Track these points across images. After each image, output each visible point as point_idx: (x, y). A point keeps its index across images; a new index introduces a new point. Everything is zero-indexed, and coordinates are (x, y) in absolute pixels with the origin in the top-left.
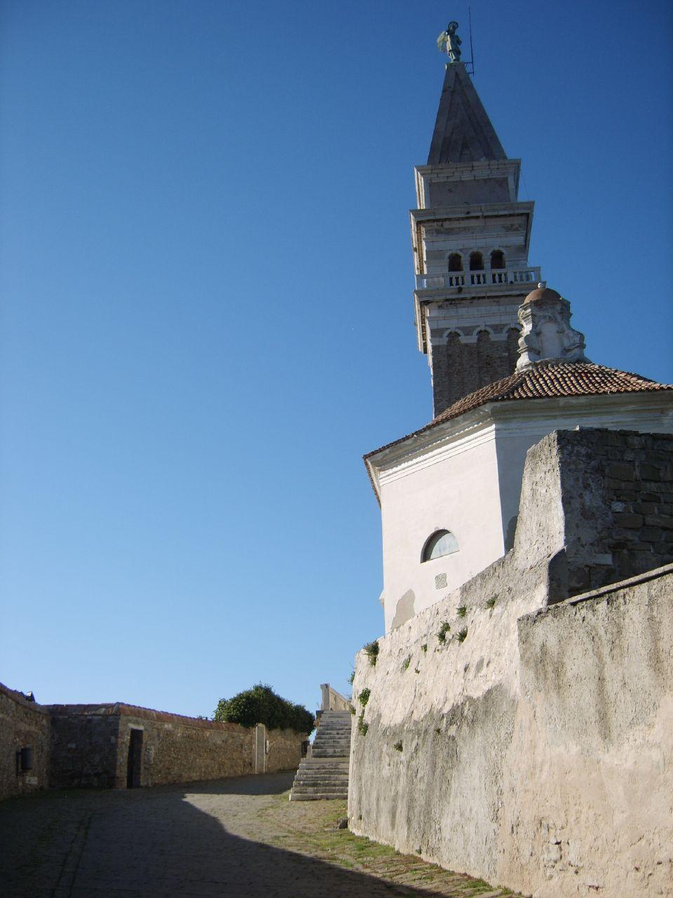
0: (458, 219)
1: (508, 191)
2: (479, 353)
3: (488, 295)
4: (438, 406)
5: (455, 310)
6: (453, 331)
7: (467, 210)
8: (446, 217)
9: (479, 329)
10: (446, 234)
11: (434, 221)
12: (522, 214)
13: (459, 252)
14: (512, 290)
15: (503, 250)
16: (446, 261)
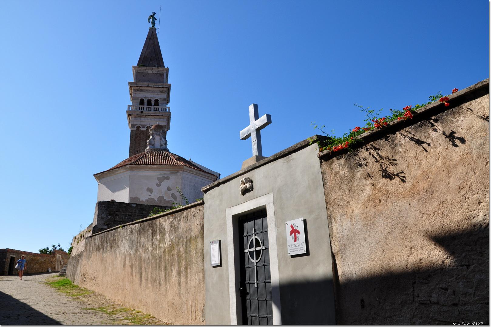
0: (145, 87)
1: (163, 78)
2: (146, 134)
3: (152, 114)
4: (131, 151)
5: (140, 118)
6: (139, 125)
7: (148, 84)
8: (140, 85)
9: (147, 126)
10: (140, 91)
11: (136, 86)
12: (166, 88)
13: (144, 98)
14: (160, 114)
15: (158, 99)
16: (139, 101)
